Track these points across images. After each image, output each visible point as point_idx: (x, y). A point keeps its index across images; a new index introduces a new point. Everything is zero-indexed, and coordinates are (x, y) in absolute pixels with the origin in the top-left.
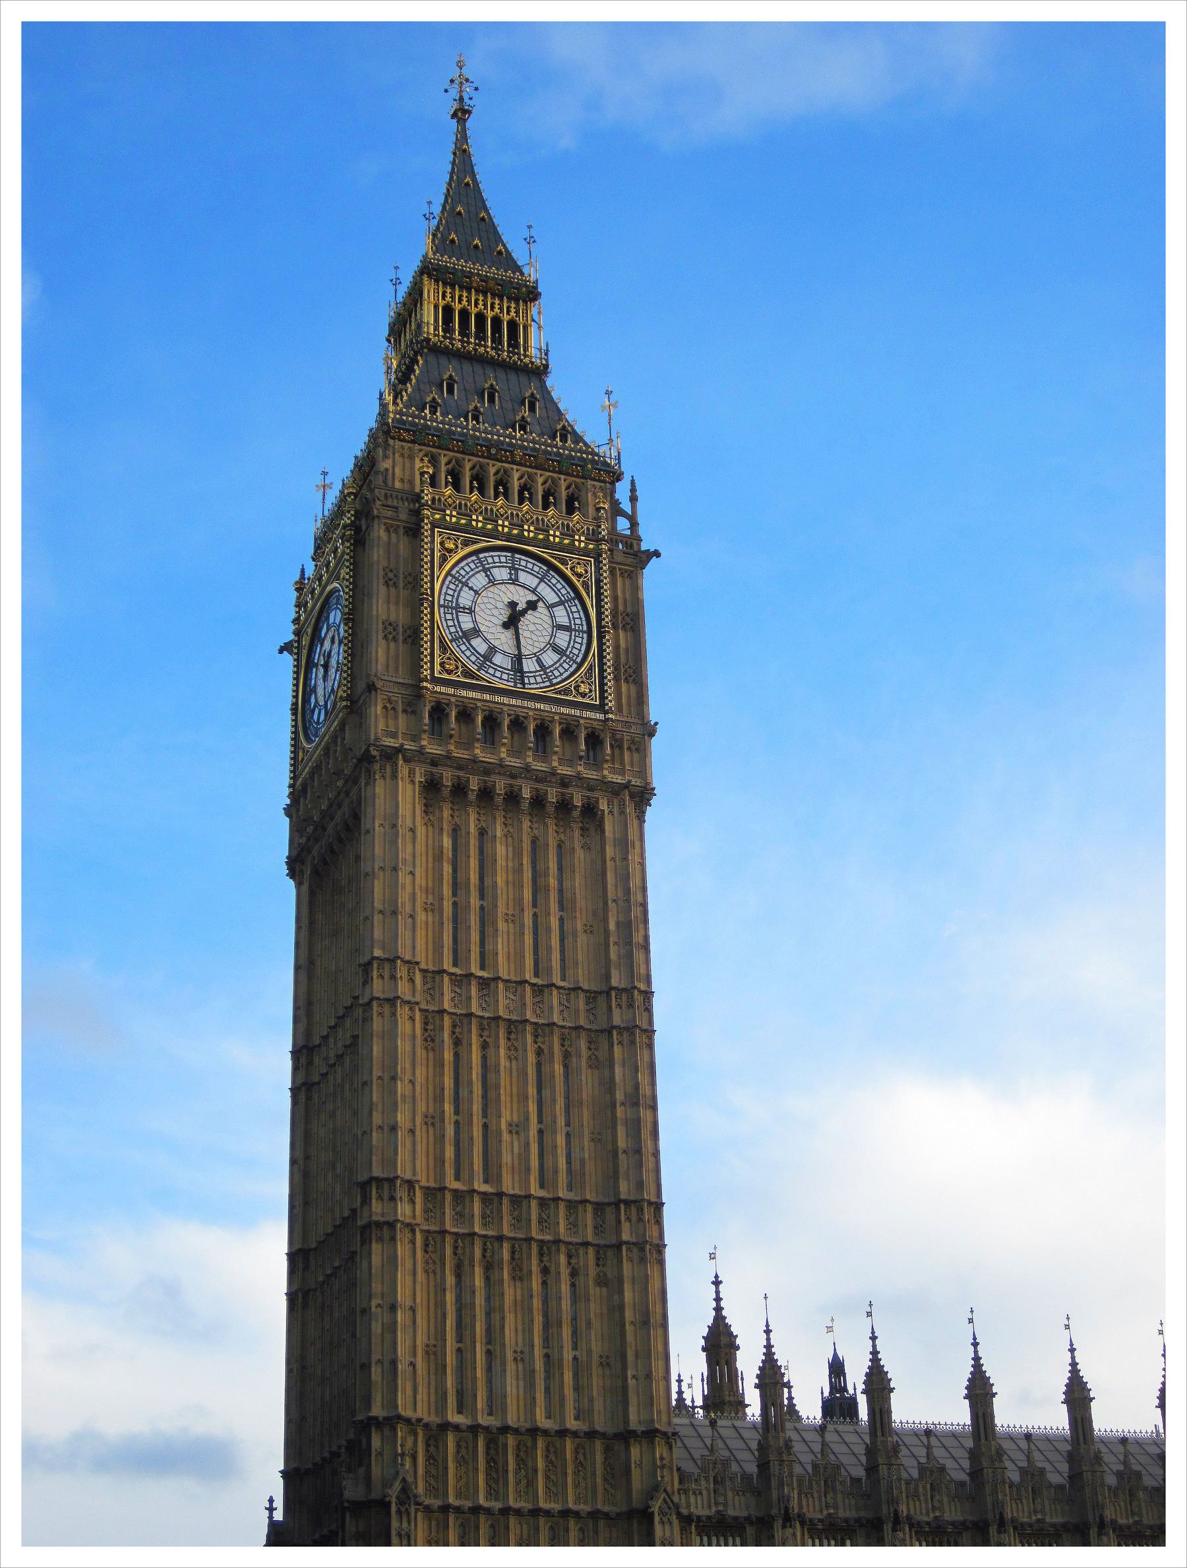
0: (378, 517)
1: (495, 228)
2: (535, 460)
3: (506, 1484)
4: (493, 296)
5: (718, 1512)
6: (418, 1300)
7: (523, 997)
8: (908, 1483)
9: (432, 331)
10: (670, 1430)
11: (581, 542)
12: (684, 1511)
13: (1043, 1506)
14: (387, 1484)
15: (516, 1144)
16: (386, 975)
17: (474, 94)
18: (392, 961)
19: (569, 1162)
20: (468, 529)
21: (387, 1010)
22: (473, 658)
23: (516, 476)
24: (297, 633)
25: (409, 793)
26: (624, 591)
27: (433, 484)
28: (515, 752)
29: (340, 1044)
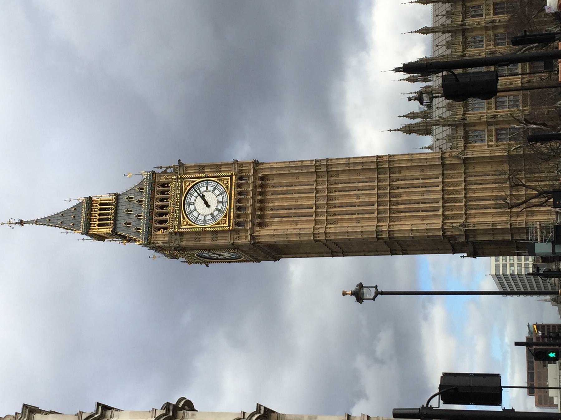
0: (179, 244)
3: (458, 197)
4: (92, 211)
5: (463, 138)
7: (320, 196)
9: (107, 230)
10: (441, 153)
13: (457, 42)
14: (461, 230)
16: (318, 236)
18: (314, 234)
21: (327, 235)
22: (220, 215)
23: (157, 203)
25: (264, 231)
26: (192, 170)
27: (165, 228)
28: (247, 200)
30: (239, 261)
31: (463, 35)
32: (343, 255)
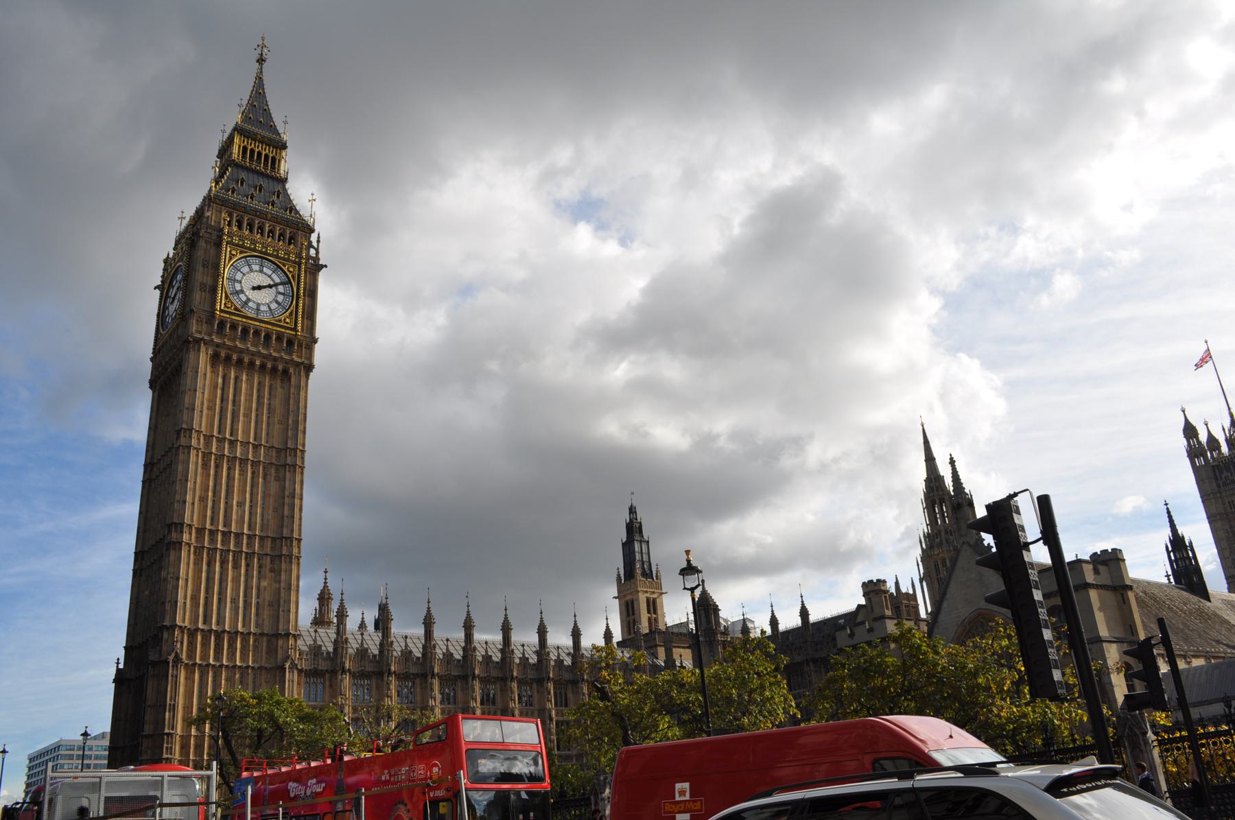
1: (270, 114)
2: (276, 220)
4: (266, 145)
5: (314, 668)
6: (190, 576)
7: (248, 449)
8: (395, 658)
9: (236, 156)
11: (292, 257)
12: (299, 667)
15: (239, 511)
16: (187, 436)
17: (268, 53)
19: (262, 520)
20: (242, 246)
22: (239, 303)
23: (267, 225)
24: (162, 282)
27: (229, 224)
29: (165, 463)
30: (158, 323)
31: (459, 676)
32: (146, 481)
